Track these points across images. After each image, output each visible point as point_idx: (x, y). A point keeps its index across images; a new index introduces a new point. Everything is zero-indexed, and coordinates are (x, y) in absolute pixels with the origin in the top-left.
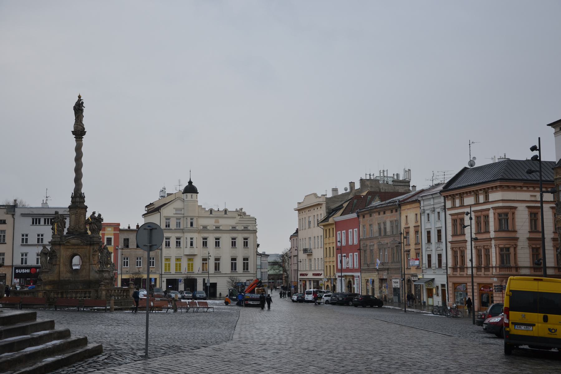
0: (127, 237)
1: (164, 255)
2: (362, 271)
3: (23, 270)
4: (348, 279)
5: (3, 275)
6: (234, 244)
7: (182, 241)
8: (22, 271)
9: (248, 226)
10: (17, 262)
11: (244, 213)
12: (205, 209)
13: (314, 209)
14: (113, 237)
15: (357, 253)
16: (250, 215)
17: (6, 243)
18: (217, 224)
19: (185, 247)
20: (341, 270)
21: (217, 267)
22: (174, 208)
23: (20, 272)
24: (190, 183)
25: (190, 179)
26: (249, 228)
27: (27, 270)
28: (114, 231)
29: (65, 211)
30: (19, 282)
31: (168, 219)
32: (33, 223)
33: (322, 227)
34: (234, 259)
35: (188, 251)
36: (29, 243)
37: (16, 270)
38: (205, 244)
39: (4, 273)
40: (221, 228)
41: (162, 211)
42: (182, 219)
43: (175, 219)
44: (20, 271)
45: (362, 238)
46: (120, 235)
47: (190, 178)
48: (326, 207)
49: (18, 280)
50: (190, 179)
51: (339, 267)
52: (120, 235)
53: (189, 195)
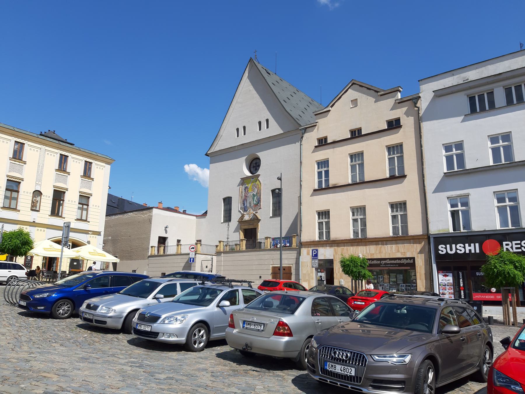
3: (460, 246)
5: (409, 261)
8: (456, 249)
23: (449, 252)
27: (470, 246)
30: (451, 281)
32: (473, 110)
36: (469, 165)
37: (440, 247)
39: (408, 255)
44: (451, 250)
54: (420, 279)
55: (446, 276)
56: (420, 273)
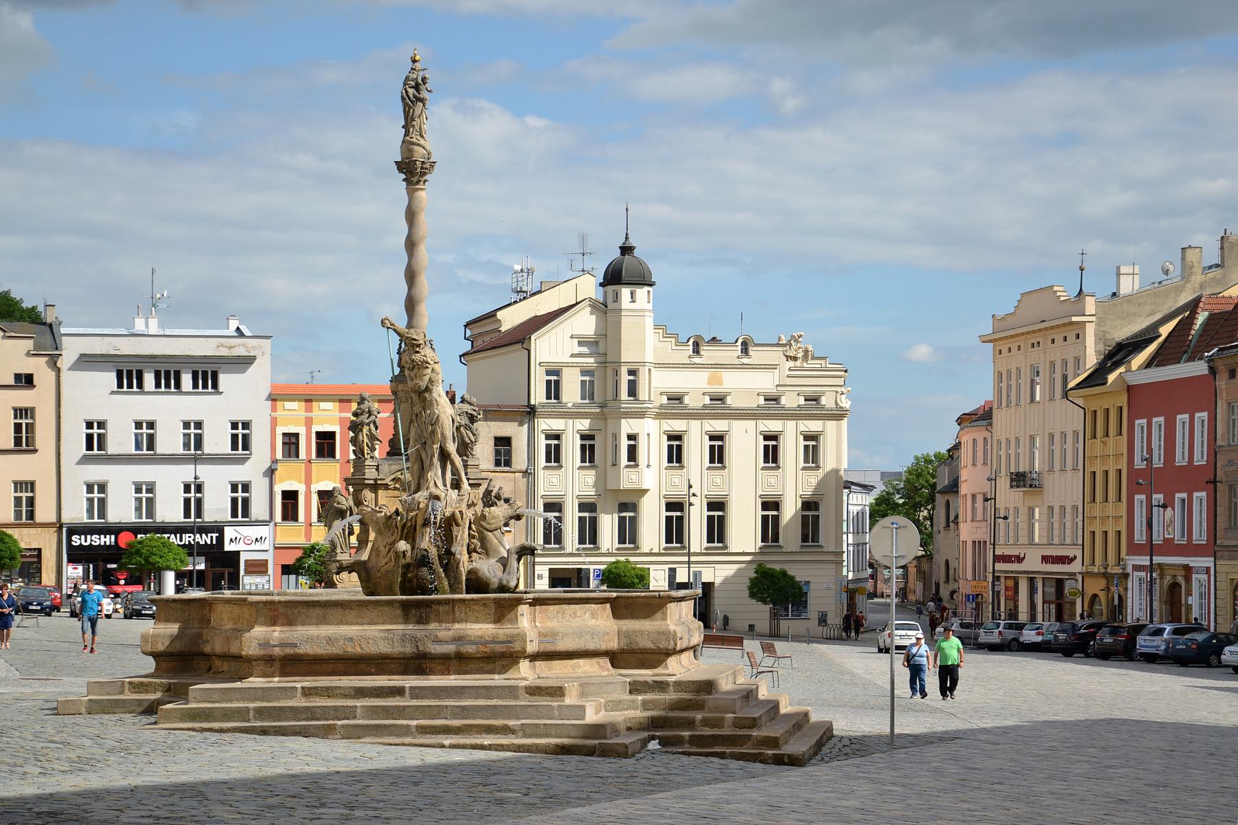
1: (541, 491)
2: (1218, 554)
4: (1168, 578)
6: (771, 455)
7: (598, 443)
8: (92, 540)
9: (824, 392)
10: (76, 512)
13: (1053, 341)
15: (1204, 494)
17: (37, 451)
18: (717, 389)
19: (609, 462)
20: (1151, 549)
21: (717, 530)
24: (626, 250)
25: (626, 238)
27: (105, 537)
29: (222, 346)
30: (81, 574)
31: (554, 372)
32: (120, 385)
33: (1080, 402)
34: (771, 504)
38: (675, 455)
44: (86, 541)
45: (1223, 444)
47: (627, 234)
48: (1096, 335)
49: (80, 568)
51: (1140, 536)
54: (47, 573)
55: (75, 568)
56: (47, 566)
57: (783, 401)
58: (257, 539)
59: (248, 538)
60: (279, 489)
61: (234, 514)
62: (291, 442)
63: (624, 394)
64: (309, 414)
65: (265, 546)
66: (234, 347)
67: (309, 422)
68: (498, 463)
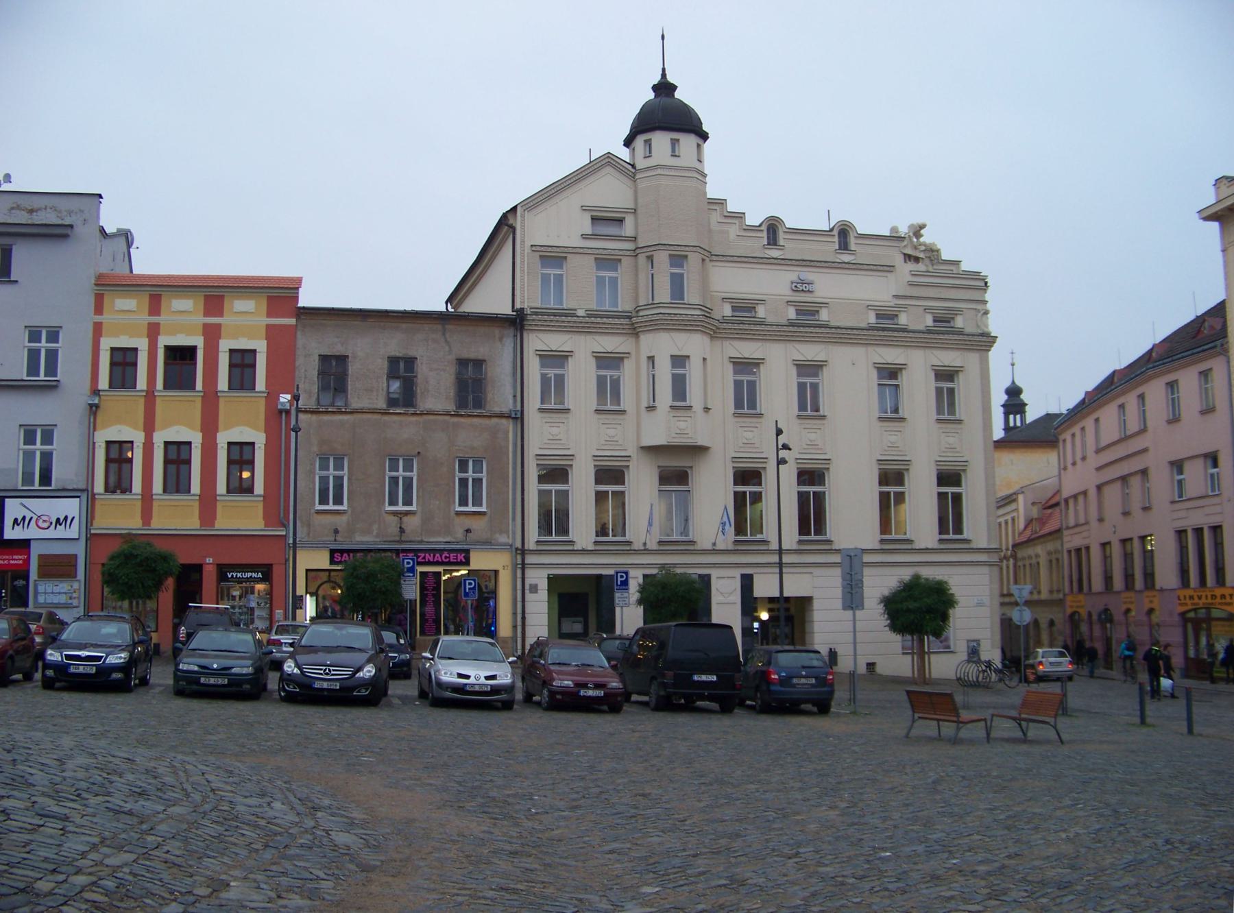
0: (338, 350)
9: (960, 310)
11: (932, 253)
12: (740, 216)
14: (261, 346)
16: (957, 263)
22: (584, 209)
24: (664, 88)
25: (664, 75)
26: (959, 322)
28: (269, 315)
29: (18, 207)
35: (660, 430)
40: (824, 315)
41: (523, 216)
42: (626, 262)
43: (590, 261)
46: (299, 334)
47: (664, 70)
50: (664, 75)
52: (301, 340)
53: (661, 140)
57: (903, 319)
58: (58, 520)
59: (44, 518)
60: (101, 437)
61: (28, 478)
62: (124, 361)
63: (664, 294)
64: (154, 319)
65: (73, 532)
66: (37, 211)
67: (153, 332)
68: (462, 402)
